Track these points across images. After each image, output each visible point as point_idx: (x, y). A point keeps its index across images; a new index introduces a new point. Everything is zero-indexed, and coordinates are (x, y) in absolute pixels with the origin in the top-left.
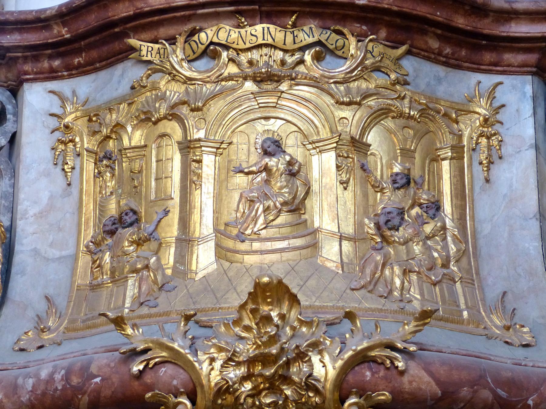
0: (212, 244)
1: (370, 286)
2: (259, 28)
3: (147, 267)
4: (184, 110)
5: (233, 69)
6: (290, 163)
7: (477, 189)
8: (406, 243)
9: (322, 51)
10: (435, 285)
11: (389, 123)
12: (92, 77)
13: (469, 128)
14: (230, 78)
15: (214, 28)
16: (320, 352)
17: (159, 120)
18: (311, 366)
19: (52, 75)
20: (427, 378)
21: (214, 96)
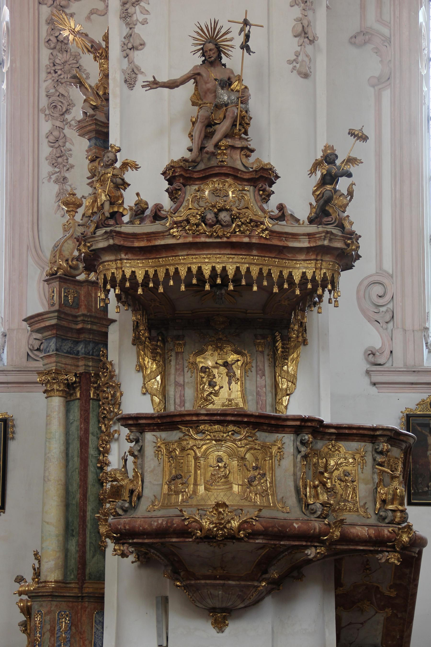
0: (203, 486)
1: (246, 499)
2: (216, 426)
3: (185, 491)
4: (195, 447)
5: (209, 437)
6: (225, 464)
7: (276, 467)
8: (256, 486)
9: (234, 432)
10: (263, 497)
11: (252, 451)
12: (166, 432)
13: (274, 450)
14: (208, 440)
15: (204, 426)
16: (234, 521)
17: (187, 450)
18: (232, 524)
19: (153, 430)
20: (260, 526)
21: (203, 445)
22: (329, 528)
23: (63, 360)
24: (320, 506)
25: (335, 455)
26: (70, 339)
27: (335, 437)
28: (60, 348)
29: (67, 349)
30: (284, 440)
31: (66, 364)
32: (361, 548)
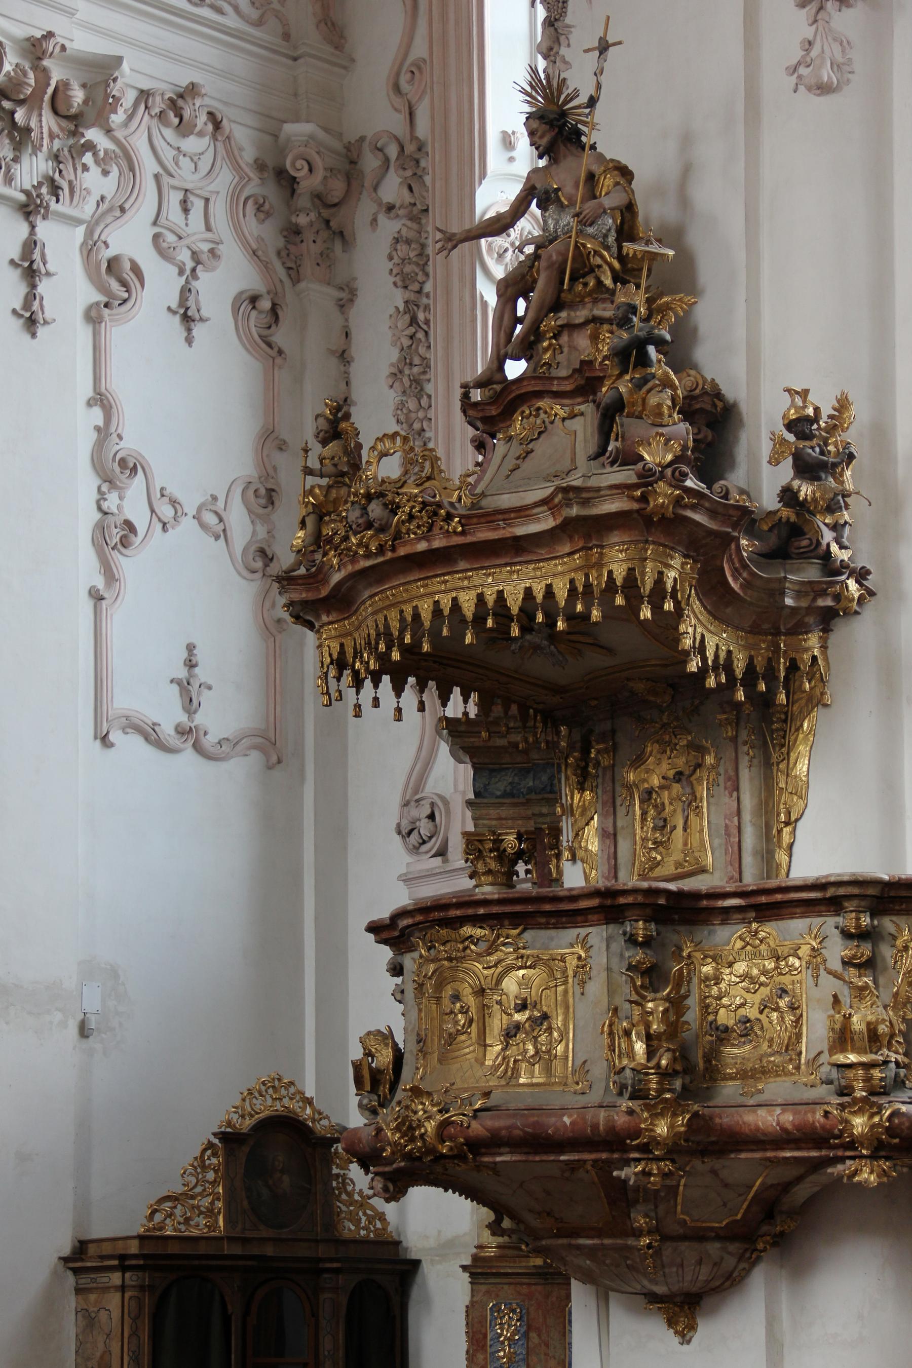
6: (462, 1007)
23: (492, 812)
26: (508, 769)
27: (753, 914)
28: (486, 790)
29: (502, 789)
30: (592, 940)
31: (500, 819)
32: (788, 1154)
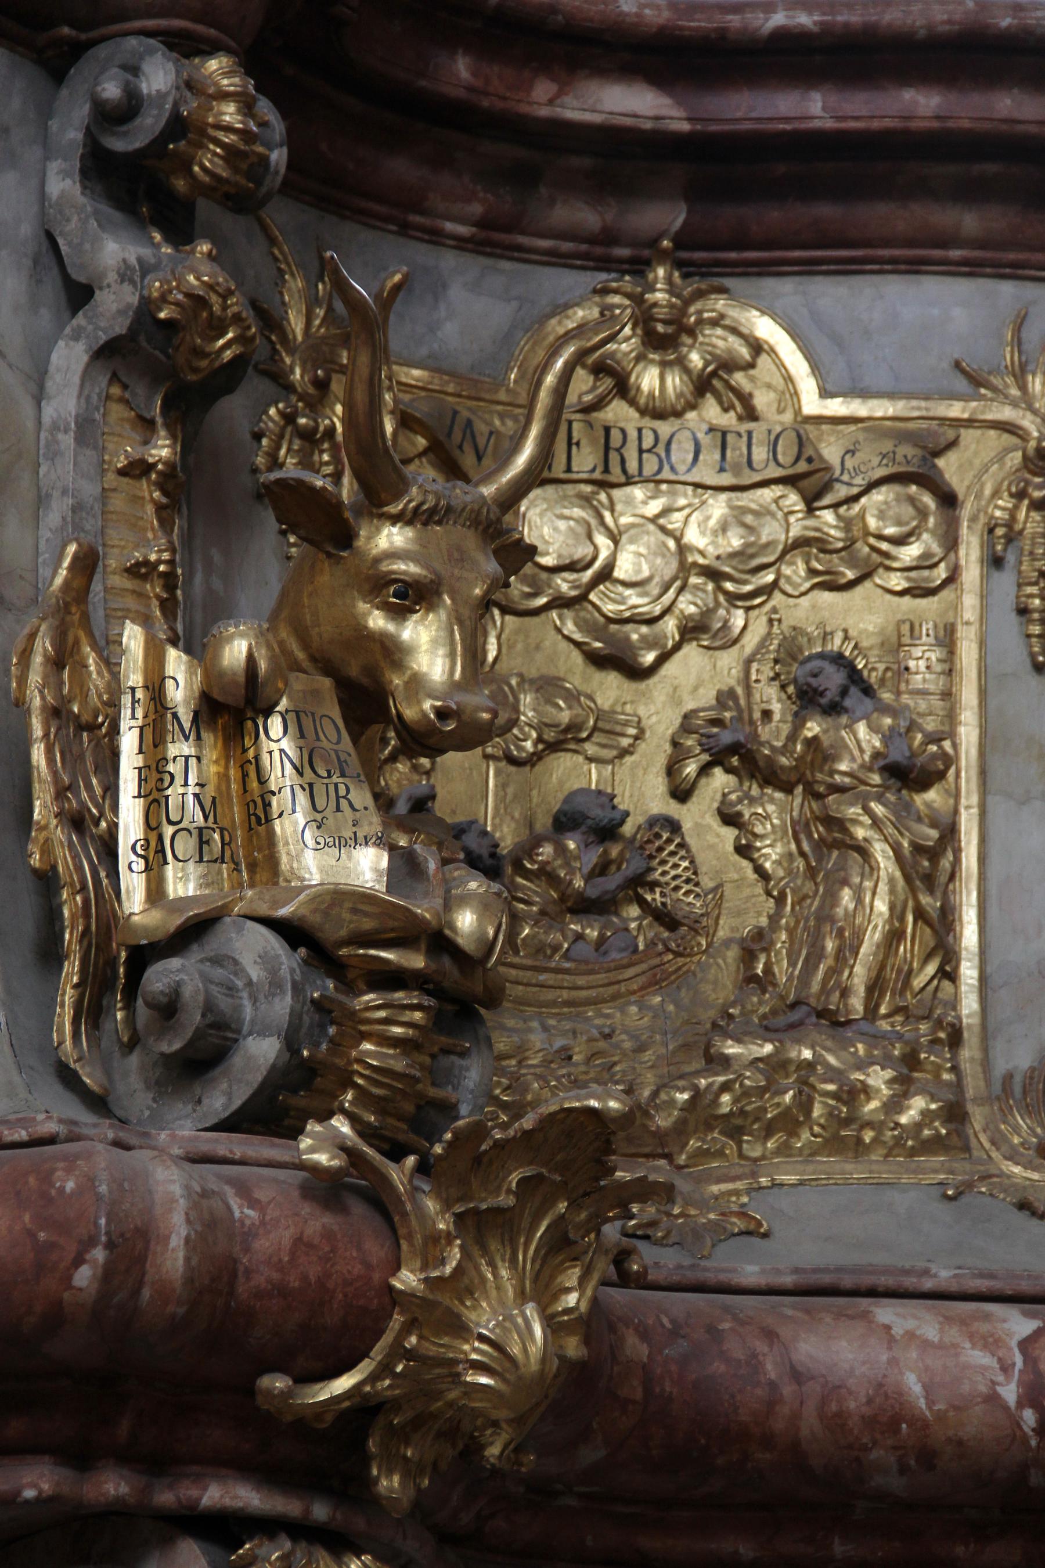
22: (376, 1250)
24: (265, 959)
25: (682, 454)
